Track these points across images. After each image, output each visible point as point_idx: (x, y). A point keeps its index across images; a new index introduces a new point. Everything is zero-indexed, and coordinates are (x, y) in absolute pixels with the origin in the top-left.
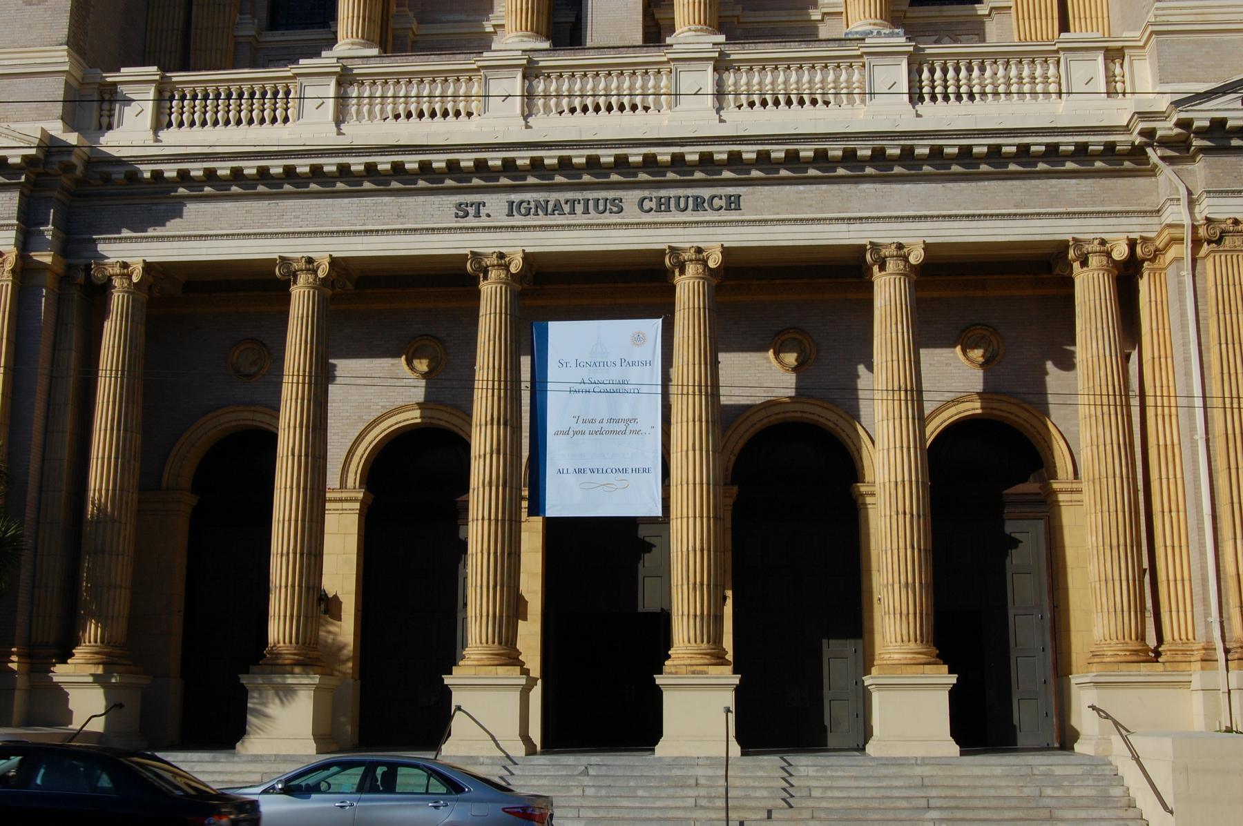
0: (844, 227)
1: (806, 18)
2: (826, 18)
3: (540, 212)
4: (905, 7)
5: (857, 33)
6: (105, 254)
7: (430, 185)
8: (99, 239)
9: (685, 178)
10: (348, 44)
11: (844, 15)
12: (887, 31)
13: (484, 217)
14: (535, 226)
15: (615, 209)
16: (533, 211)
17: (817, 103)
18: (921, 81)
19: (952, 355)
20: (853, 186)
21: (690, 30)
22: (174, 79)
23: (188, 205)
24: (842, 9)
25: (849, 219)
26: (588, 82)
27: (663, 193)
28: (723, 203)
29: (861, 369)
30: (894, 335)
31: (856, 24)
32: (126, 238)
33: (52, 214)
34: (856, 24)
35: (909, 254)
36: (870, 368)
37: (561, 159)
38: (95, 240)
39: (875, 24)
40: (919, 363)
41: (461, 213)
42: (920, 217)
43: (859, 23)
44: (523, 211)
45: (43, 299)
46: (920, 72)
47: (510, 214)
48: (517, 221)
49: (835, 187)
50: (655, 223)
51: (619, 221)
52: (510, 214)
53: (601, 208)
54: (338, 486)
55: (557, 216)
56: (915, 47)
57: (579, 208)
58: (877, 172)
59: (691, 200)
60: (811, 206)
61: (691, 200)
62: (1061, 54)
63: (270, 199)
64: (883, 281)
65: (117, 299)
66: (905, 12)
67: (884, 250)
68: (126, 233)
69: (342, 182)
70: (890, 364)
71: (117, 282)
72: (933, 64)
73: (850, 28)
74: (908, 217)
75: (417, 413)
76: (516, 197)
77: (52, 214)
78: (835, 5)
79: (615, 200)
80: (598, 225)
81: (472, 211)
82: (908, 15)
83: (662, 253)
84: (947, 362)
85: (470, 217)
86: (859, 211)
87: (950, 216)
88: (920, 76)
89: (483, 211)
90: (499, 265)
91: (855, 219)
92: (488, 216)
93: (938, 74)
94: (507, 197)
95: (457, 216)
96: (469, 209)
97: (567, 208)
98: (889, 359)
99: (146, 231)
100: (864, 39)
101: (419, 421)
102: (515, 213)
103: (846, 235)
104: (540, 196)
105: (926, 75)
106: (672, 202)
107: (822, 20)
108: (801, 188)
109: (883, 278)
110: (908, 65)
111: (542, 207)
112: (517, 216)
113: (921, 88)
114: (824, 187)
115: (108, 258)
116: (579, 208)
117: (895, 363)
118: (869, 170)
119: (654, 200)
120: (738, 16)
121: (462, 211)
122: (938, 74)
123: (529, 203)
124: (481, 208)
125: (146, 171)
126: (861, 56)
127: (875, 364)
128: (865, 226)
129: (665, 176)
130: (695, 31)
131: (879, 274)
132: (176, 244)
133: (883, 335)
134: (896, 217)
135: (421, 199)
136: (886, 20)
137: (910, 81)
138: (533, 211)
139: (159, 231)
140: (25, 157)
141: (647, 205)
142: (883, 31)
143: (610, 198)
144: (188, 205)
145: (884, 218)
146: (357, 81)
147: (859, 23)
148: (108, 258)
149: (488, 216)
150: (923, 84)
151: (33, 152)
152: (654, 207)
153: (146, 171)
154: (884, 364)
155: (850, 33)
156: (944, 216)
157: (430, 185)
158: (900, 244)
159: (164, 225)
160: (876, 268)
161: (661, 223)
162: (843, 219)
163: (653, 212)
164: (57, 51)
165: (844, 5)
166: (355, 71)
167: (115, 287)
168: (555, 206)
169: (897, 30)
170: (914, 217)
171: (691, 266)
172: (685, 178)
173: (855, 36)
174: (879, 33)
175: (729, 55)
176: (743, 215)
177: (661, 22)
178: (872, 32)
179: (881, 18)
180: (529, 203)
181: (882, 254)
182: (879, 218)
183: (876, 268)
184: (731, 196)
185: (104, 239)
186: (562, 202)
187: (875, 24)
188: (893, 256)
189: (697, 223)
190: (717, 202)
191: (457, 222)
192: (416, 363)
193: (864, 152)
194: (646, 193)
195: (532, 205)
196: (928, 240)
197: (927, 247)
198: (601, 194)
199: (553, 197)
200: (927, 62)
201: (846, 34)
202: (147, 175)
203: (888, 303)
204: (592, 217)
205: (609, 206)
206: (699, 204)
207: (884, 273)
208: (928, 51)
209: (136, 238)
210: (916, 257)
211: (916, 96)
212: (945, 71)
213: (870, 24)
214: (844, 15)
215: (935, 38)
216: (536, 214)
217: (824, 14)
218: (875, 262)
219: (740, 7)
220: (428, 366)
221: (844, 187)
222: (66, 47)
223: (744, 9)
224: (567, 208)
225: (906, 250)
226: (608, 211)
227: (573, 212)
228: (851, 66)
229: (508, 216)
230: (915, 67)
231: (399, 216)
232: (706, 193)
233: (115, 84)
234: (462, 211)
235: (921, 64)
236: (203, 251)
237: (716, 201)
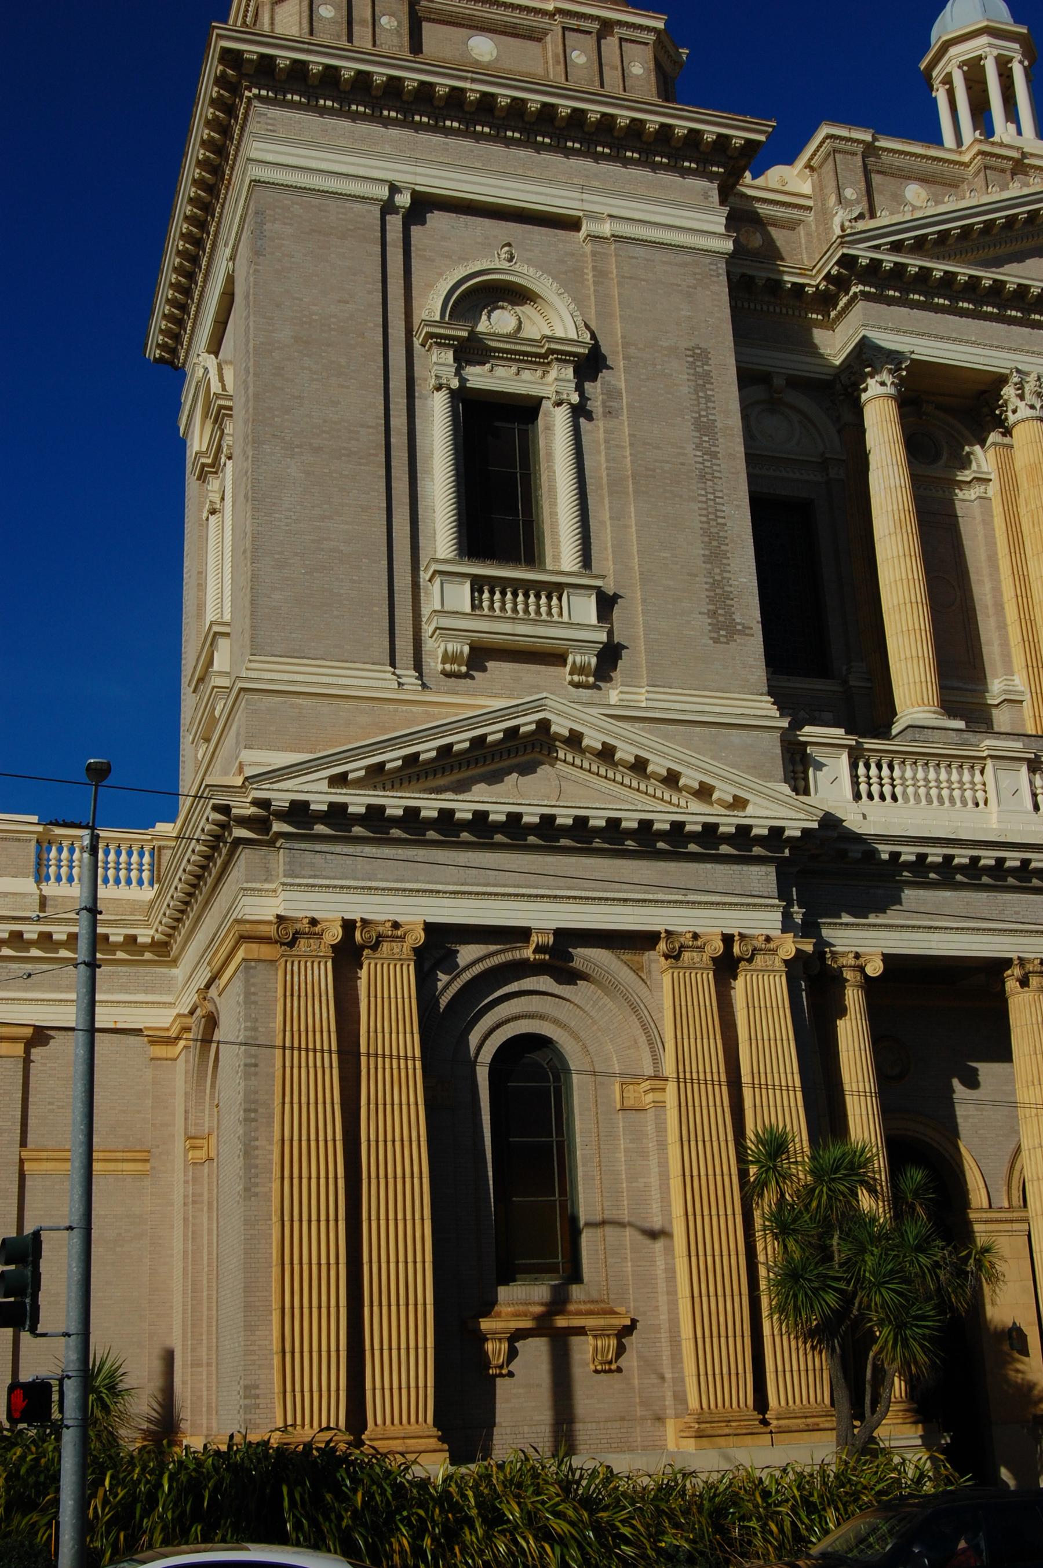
6: (831, 940)
8: (824, 923)
22: (866, 746)
23: (906, 891)
32: (847, 924)
33: (794, 893)
38: (819, 923)
45: (804, 993)
54: (1006, 1205)
63: (989, 891)
65: (853, 997)
68: (846, 919)
71: (848, 974)
77: (794, 893)
99: (867, 918)
115: (834, 946)
125: (885, 852)
132: (906, 935)
139: (881, 920)
140: (805, 831)
144: (906, 891)
148: (834, 946)
151: (815, 825)
153: (885, 852)
159: (885, 913)
164: (761, 701)
167: (848, 981)
185: (830, 924)
202: (885, 856)
209: (858, 925)
222: (769, 698)
233: (806, 744)
236: (934, 945)
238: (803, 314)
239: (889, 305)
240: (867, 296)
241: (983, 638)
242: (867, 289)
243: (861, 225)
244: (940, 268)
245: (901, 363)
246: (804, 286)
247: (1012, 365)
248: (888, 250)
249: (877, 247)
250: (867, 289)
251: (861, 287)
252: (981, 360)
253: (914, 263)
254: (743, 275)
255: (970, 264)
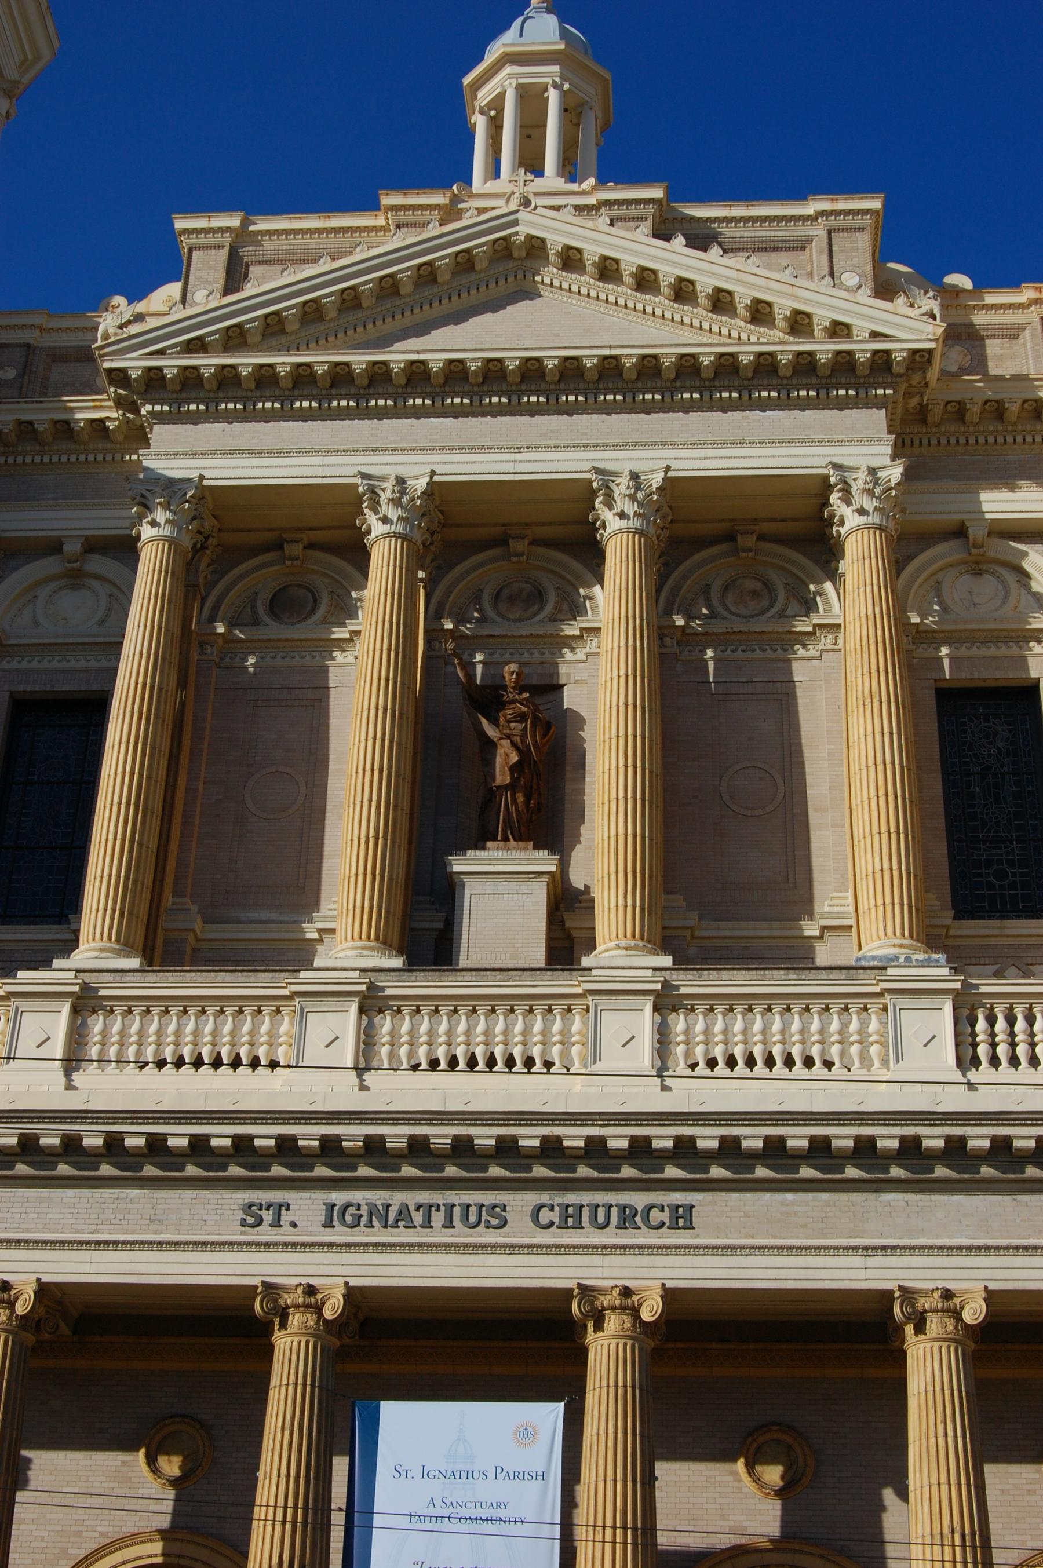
0: (856, 1261)
1: (795, 933)
2: (827, 933)
3: (375, 1222)
4: (948, 921)
5: (874, 958)
7: (206, 1174)
9: (607, 1175)
10: (94, 949)
11: (854, 929)
12: (921, 956)
13: (286, 1228)
14: (366, 1245)
15: (494, 1222)
16: (364, 1220)
17: (716, 1064)
18: (974, 1035)
19: (1037, 1475)
20: (871, 1196)
21: (618, 947)
24: (851, 922)
25: (866, 1248)
26: (225, 1023)
27: (571, 1198)
28: (665, 1217)
29: (889, 1495)
30: (941, 1441)
31: (872, 945)
34: (872, 945)
35: (962, 1308)
36: (903, 1494)
37: (237, 1138)
39: (901, 946)
40: (983, 1488)
41: (250, 1220)
42: (979, 1248)
43: (878, 943)
44: (349, 1219)
46: (973, 1022)
47: (329, 1224)
48: (340, 1234)
49: (843, 1197)
50: (558, 1246)
51: (501, 1240)
52: (329, 1224)
53: (473, 1219)
55: (402, 1229)
56: (963, 982)
57: (438, 1218)
58: (909, 1175)
59: (614, 1211)
60: (804, 1226)
61: (614, 1211)
62: (888, 999)
64: (921, 1351)
66: (948, 927)
67: (922, 1301)
69: (66, 1163)
70: (935, 1489)
72: (992, 1009)
73: (864, 949)
74: (960, 1248)
75: (157, 1547)
76: (338, 1197)
78: (840, 915)
79: (494, 1207)
80: (466, 1246)
81: (268, 1216)
82: (952, 932)
83: (250, 1291)
84: (1029, 1487)
85: (265, 1227)
86: (882, 1236)
87: (1026, 1248)
88: (973, 1026)
89: (286, 1217)
90: (307, 1306)
91: (875, 1248)
92: (294, 1225)
93: (1001, 1025)
94: (324, 1196)
95: (244, 1223)
96: (264, 1213)
97: (418, 1218)
98: (934, 1481)
100: (885, 968)
101: (159, 1560)
102: (336, 1222)
103: (861, 1274)
104: (377, 1197)
105: (981, 1025)
106: (586, 1212)
107: (821, 937)
108: (790, 1196)
109: (922, 1346)
110: (954, 1009)
111: (379, 1215)
112: (339, 1228)
113: (975, 1045)
114: (825, 1196)
116: (438, 1218)
117: (944, 1488)
118: (896, 1172)
119: (556, 1208)
120: (692, 928)
121: (252, 1216)
122: (1001, 1025)
123: (359, 1207)
124: (283, 1212)
126: (880, 994)
127: (911, 1488)
128: (892, 1261)
129: (575, 1171)
130: (626, 949)
131: (914, 1339)
133: (924, 1441)
134: (941, 1248)
135: (188, 1194)
136: (918, 940)
137: (957, 1035)
138: (364, 1220)
141: (545, 1216)
142: (914, 957)
143: (486, 1203)
145: (922, 1248)
146: (104, 1008)
147: (878, 943)
149: (294, 1225)
150: (978, 1039)
152: (556, 1220)
154: (926, 1489)
155: (864, 958)
156: (1017, 1248)
157: (206, 1174)
158: (948, 1290)
160: (909, 1330)
161: (567, 1247)
162: (855, 1248)
163: (554, 1229)
165: (854, 914)
166: (102, 992)
168: (400, 1213)
169: (935, 956)
170: (969, 1248)
171: (297, 1315)
172: (607, 1175)
173: (872, 964)
174: (908, 959)
175: (678, 987)
176: (697, 1236)
177: (574, 933)
178: (897, 958)
179: (911, 936)
180: (359, 1207)
181: (919, 1306)
182: (912, 1248)
183: (909, 1330)
184: (678, 1207)
186: (412, 1208)
187: (901, 946)
188: (936, 1311)
189: (624, 1247)
190: (656, 1216)
191: (243, 1233)
192: (162, 1461)
193: (50, 1140)
194: (545, 1198)
195: (364, 1211)
196: (993, 1286)
197: (991, 1297)
198: (474, 1197)
199: (398, 1198)
200: (983, 1005)
201: (858, 959)
203: (930, 1388)
204: (459, 1234)
205: (485, 1216)
206: (627, 1218)
207: (922, 1337)
208: (983, 989)
210: (974, 1312)
211: (967, 1060)
212: (1011, 1021)
213: (894, 946)
214: (854, 929)
215: (996, 967)
216: (370, 1225)
217: (824, 928)
218: (908, 1319)
219: (695, 915)
220: (181, 1468)
221: (857, 1197)
223: (701, 918)
224: (418, 1218)
225: (957, 1301)
226: (483, 1224)
227: (427, 1224)
228: (866, 1009)
229: (324, 1226)
230: (965, 1012)
231: (152, 1221)
232: (638, 1200)
234: (252, 1216)
235: (973, 1009)
237: (655, 1214)
238: (118, 457)
239: (196, 424)
240: (162, 418)
241: (327, 849)
242: (157, 408)
243: (135, 329)
244: (283, 361)
245: (185, 494)
246: (102, 421)
247: (353, 471)
248: (178, 353)
249: (161, 352)
250: (157, 408)
251: (149, 407)
252: (319, 472)
253: (207, 363)
254: (20, 423)
255: (327, 348)
